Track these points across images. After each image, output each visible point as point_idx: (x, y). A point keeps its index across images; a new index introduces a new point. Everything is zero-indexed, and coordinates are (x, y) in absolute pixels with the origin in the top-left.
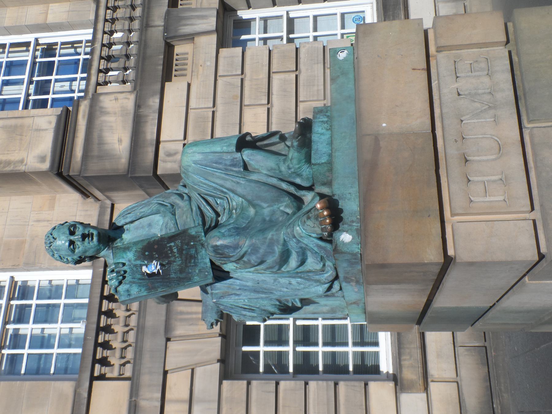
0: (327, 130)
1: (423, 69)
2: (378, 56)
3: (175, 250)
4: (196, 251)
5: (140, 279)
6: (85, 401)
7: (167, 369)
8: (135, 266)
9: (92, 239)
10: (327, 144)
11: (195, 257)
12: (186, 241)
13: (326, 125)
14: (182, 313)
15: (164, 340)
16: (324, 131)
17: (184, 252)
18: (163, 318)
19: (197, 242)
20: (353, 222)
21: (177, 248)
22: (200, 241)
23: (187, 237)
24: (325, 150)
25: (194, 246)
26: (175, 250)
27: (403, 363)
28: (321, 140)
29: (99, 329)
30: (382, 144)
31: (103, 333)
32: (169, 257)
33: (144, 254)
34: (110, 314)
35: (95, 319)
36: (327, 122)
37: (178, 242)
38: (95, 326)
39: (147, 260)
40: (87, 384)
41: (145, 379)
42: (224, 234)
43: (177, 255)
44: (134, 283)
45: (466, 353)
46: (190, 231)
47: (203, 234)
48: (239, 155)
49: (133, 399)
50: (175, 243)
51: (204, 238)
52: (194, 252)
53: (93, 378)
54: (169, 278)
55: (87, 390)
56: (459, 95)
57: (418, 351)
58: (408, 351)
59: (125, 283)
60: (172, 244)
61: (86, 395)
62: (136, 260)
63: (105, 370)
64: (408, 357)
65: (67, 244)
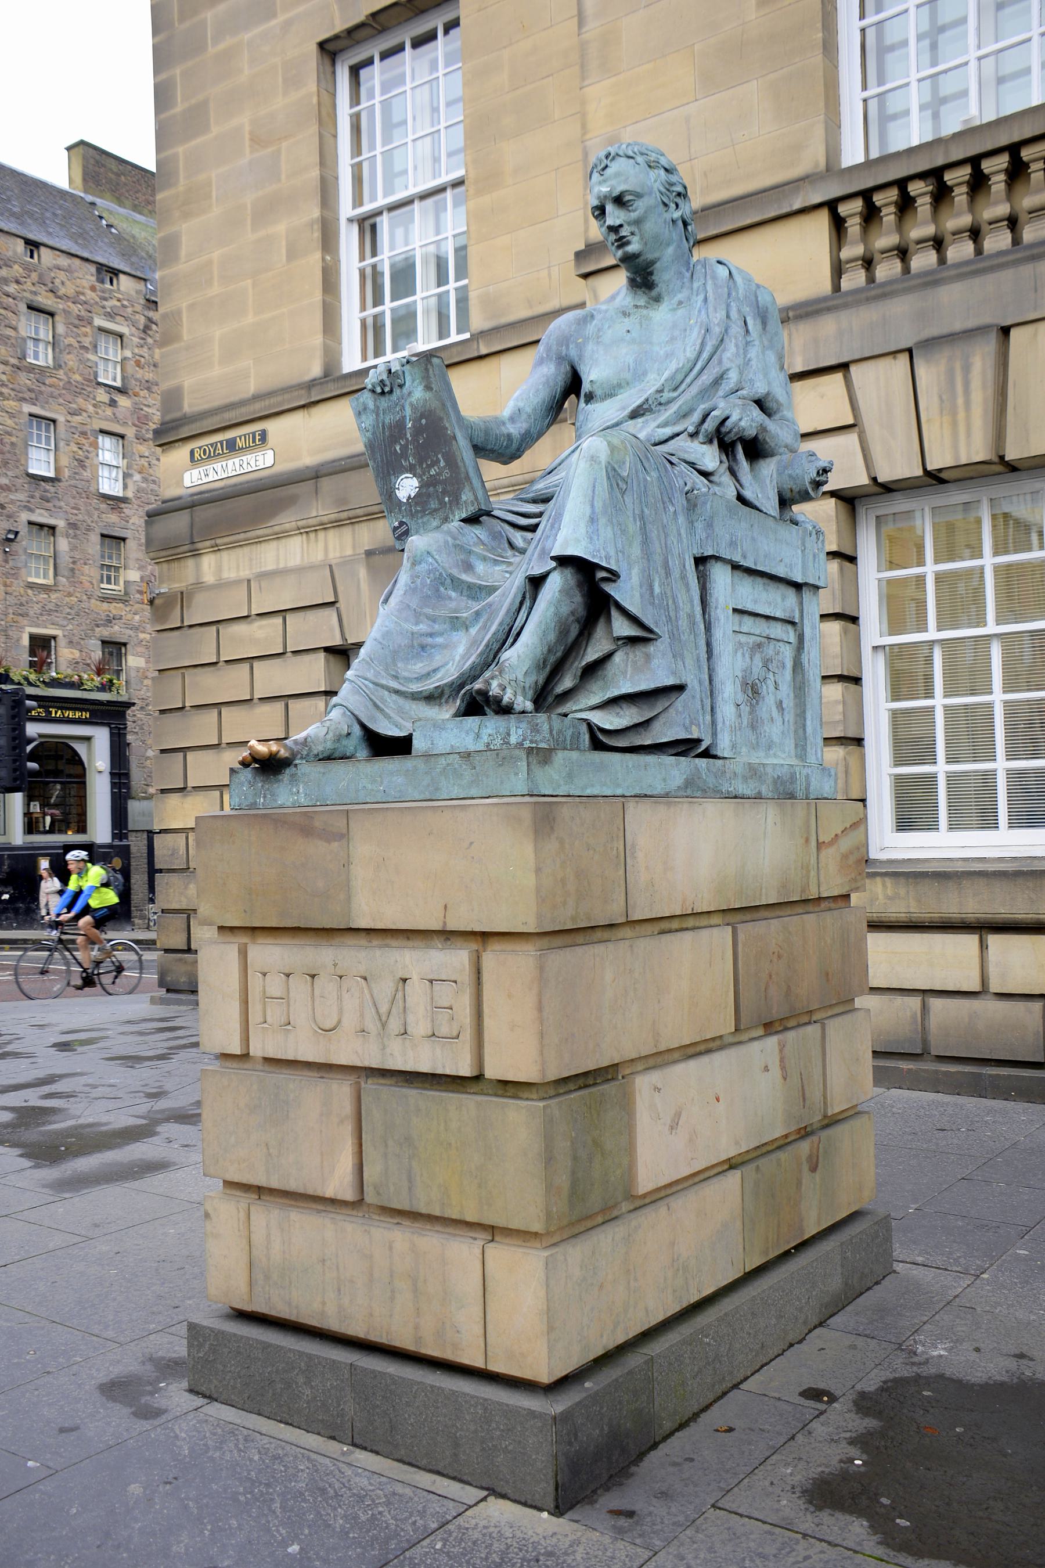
0: (488, 745)
1: (445, 923)
2: (471, 843)
3: (432, 472)
4: (436, 510)
5: (383, 423)
6: (785, 210)
7: (853, 369)
8: (403, 407)
9: (619, 247)
10: (452, 746)
11: (423, 511)
12: (448, 488)
13: (498, 742)
14: (967, 369)
15: (908, 346)
16: (485, 739)
17: (431, 489)
18: (958, 326)
19: (451, 507)
20: (265, 797)
21: (437, 474)
22: (453, 513)
23: (456, 486)
24: (441, 743)
25: (442, 503)
26: (432, 472)
27: (878, 879)
28: (464, 735)
29: (935, 174)
30: (335, 845)
31: (930, 188)
32: (421, 465)
33: (422, 416)
34: (978, 183)
35: (958, 153)
36: (508, 743)
37: (446, 474)
38: (940, 162)
39: (413, 426)
40: (817, 199)
41: (828, 326)
42: (420, 563)
43: (425, 478)
44: (377, 415)
45: (909, 1014)
46: (467, 489)
47: (464, 515)
48: (554, 564)
49: (791, 314)
50: (445, 467)
51: (457, 517)
52: (433, 506)
53: (832, 205)
54: (389, 474)
55: (807, 204)
56: (405, 980)
57: (903, 915)
58: (902, 891)
59: (375, 400)
60: (442, 464)
61: (797, 206)
62: (411, 405)
63: (854, 226)
64: (889, 892)
65: (596, 203)
